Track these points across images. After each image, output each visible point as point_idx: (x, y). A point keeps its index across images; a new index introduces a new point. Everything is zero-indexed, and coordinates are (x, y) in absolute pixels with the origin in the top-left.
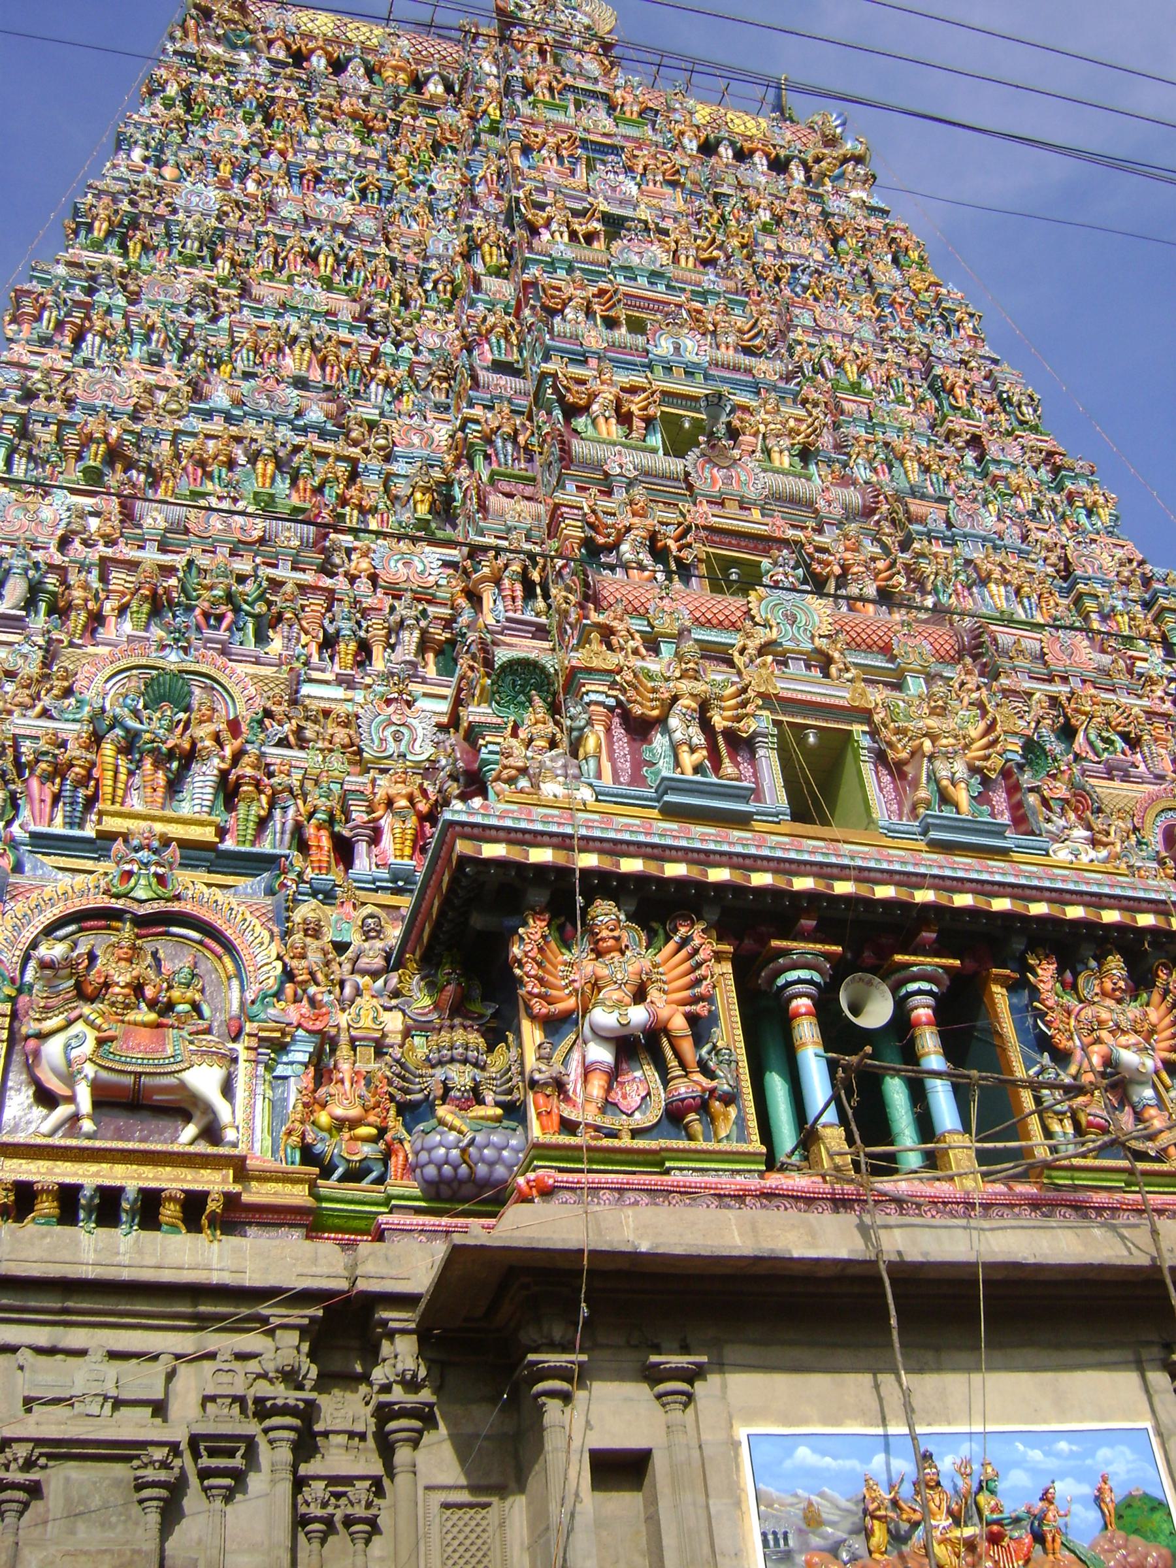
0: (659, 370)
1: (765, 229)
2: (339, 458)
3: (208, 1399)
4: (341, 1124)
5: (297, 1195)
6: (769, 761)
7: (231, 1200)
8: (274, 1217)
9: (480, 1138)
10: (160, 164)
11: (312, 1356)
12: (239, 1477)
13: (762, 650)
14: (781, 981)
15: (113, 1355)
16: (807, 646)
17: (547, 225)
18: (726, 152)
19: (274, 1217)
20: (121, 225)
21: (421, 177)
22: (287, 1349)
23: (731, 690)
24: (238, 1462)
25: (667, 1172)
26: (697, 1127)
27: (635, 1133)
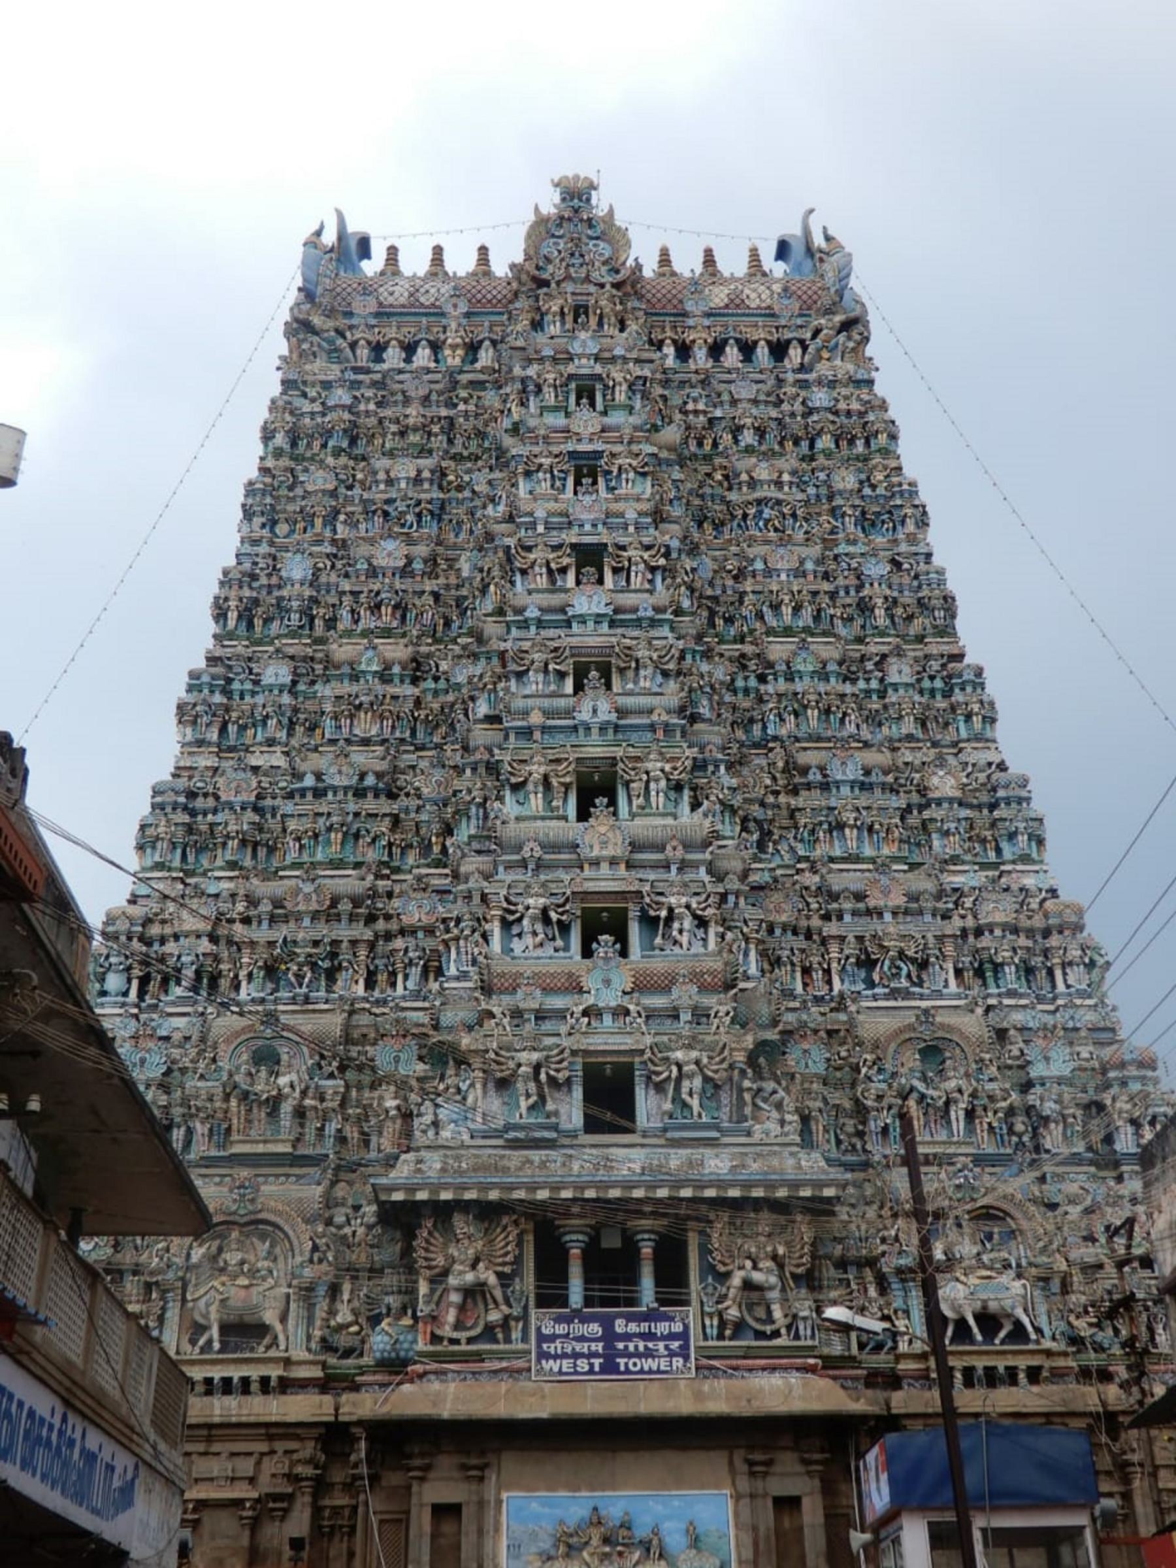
0: (581, 731)
1: (749, 450)
2: (385, 815)
3: (274, 1475)
4: (341, 1327)
5: (317, 1373)
6: (578, 1093)
7: (281, 1379)
8: (303, 1385)
9: (402, 1338)
10: (274, 523)
11: (323, 1450)
12: (286, 1511)
13: (585, 1013)
14: (567, 1238)
15: (233, 1454)
16: (613, 1004)
17: (532, 566)
18: (732, 355)
19: (303, 1385)
20: (246, 609)
21: (466, 478)
22: (308, 1449)
23: (555, 1052)
24: (285, 1505)
25: (483, 1361)
26: (500, 1336)
27: (470, 1341)
